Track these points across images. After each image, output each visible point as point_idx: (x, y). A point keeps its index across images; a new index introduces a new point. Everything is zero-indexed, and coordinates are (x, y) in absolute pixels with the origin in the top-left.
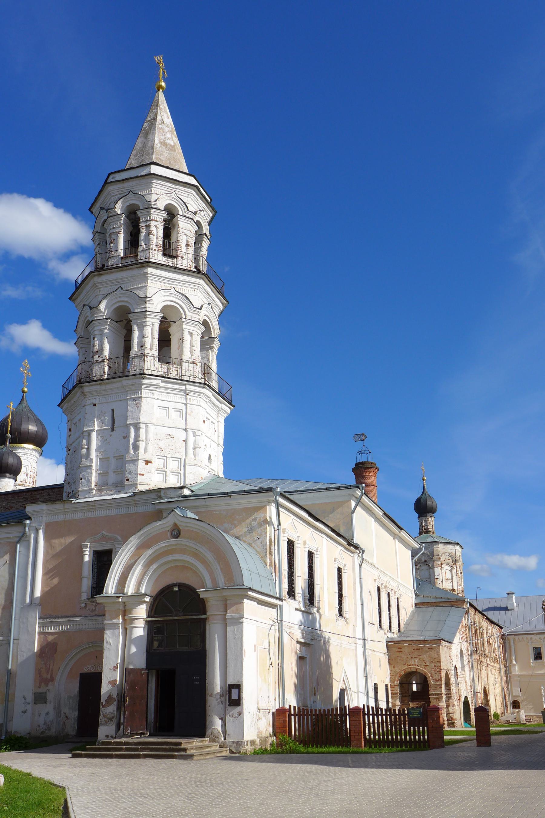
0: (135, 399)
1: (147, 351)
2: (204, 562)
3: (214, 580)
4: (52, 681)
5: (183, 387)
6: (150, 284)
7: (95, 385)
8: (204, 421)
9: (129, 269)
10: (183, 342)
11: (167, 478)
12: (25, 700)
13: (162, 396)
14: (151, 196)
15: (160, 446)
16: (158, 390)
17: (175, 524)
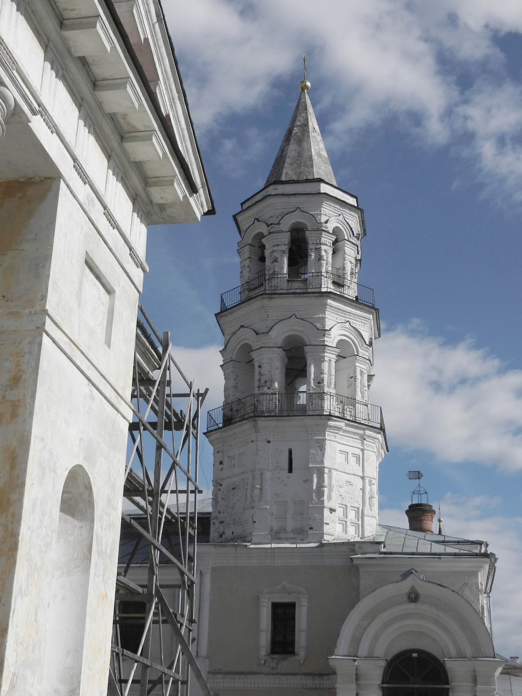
0: (317, 441)
1: (326, 390)
5: (361, 432)
6: (327, 315)
9: (305, 297)
10: (355, 381)
11: (348, 528)
13: (342, 440)
14: (321, 216)
15: (341, 494)
16: (340, 433)
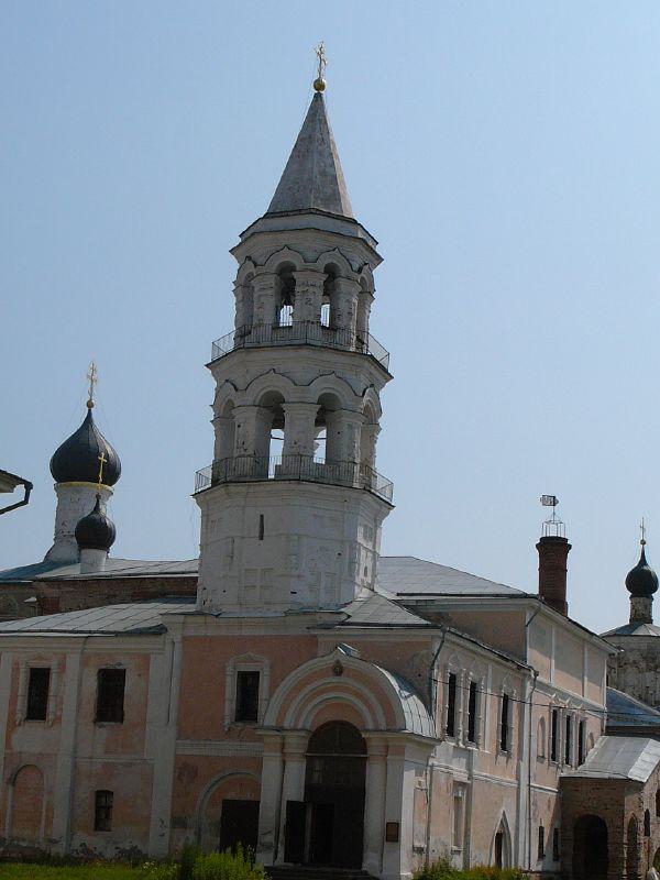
2: (366, 702)
3: (375, 721)
17: (338, 662)
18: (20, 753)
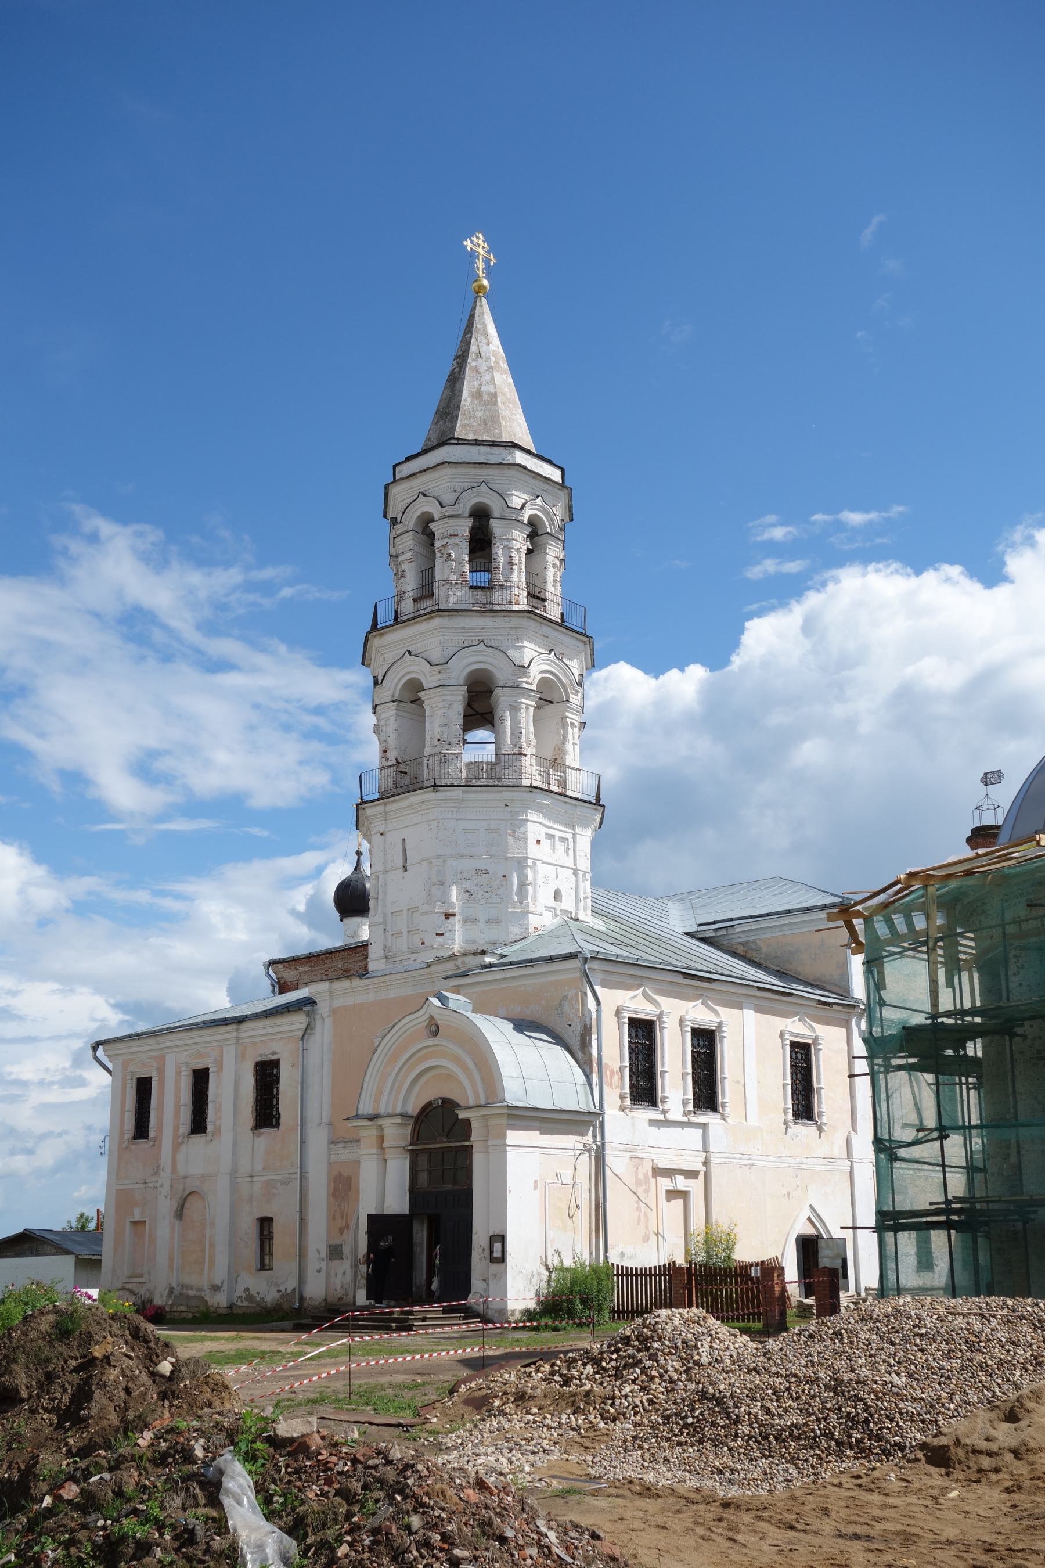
2: (465, 1069)
3: (476, 1095)
4: (348, 1229)
7: (378, 805)
8: (538, 842)
9: (416, 623)
12: (319, 1253)
18: (185, 1178)
